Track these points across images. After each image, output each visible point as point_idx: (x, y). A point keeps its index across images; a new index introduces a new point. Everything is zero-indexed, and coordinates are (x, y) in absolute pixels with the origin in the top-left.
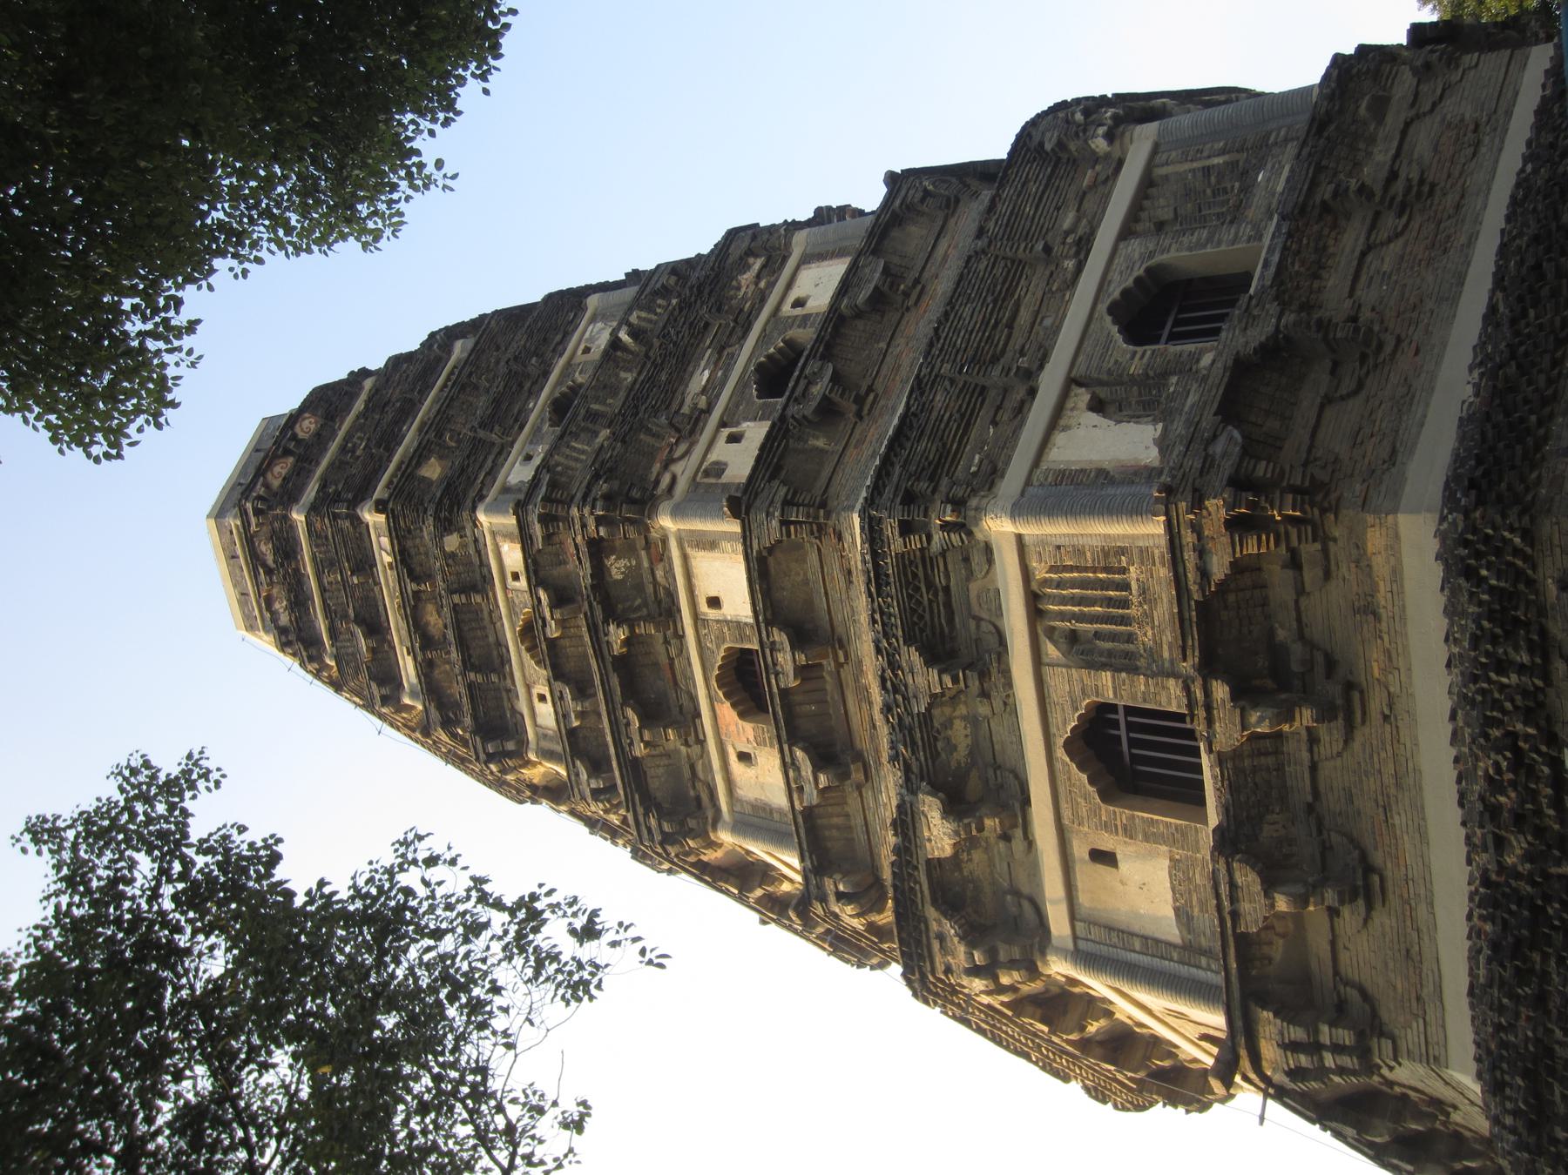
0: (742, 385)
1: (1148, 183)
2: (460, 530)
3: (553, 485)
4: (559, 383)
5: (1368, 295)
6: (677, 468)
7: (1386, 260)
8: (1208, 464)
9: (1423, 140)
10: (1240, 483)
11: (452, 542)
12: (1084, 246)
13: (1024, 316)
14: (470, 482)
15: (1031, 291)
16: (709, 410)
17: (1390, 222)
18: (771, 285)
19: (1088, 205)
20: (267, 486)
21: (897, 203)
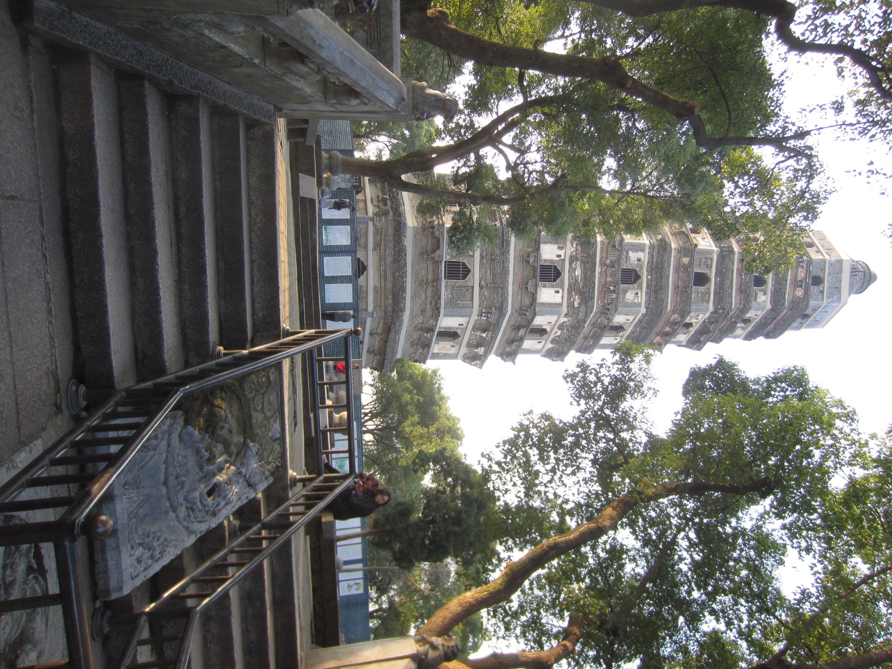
0: (563, 269)
1: (472, 300)
2: (657, 240)
3: (615, 246)
4: (641, 283)
5: (425, 265)
6: (573, 249)
7: (424, 272)
8: (438, 230)
9: (423, 297)
10: (433, 227)
11: (659, 237)
12: (481, 287)
13: (489, 271)
14: (658, 252)
15: (489, 277)
16: (570, 263)
17: (425, 279)
18: (569, 299)
19: (483, 298)
20: (802, 267)
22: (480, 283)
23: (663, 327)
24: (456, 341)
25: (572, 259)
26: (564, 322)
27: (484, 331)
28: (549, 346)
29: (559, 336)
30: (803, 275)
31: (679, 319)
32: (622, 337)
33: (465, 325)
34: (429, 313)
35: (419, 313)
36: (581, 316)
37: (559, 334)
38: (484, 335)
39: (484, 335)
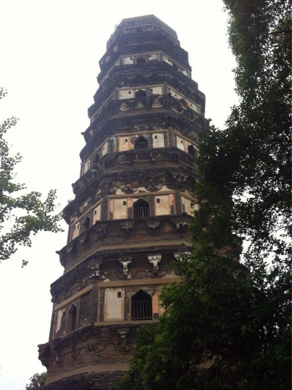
16: (81, 214)
21: (95, 228)
22: (80, 290)
23: (141, 109)
24: (150, 293)
25: (79, 215)
26: (123, 190)
27: (122, 265)
28: (164, 189)
29: (146, 187)
30: (108, 57)
31: (124, 104)
32: (151, 134)
33: (120, 290)
34: (91, 341)
35: (93, 353)
36: (109, 180)
37: (143, 189)
38: (125, 264)
39: (125, 264)
